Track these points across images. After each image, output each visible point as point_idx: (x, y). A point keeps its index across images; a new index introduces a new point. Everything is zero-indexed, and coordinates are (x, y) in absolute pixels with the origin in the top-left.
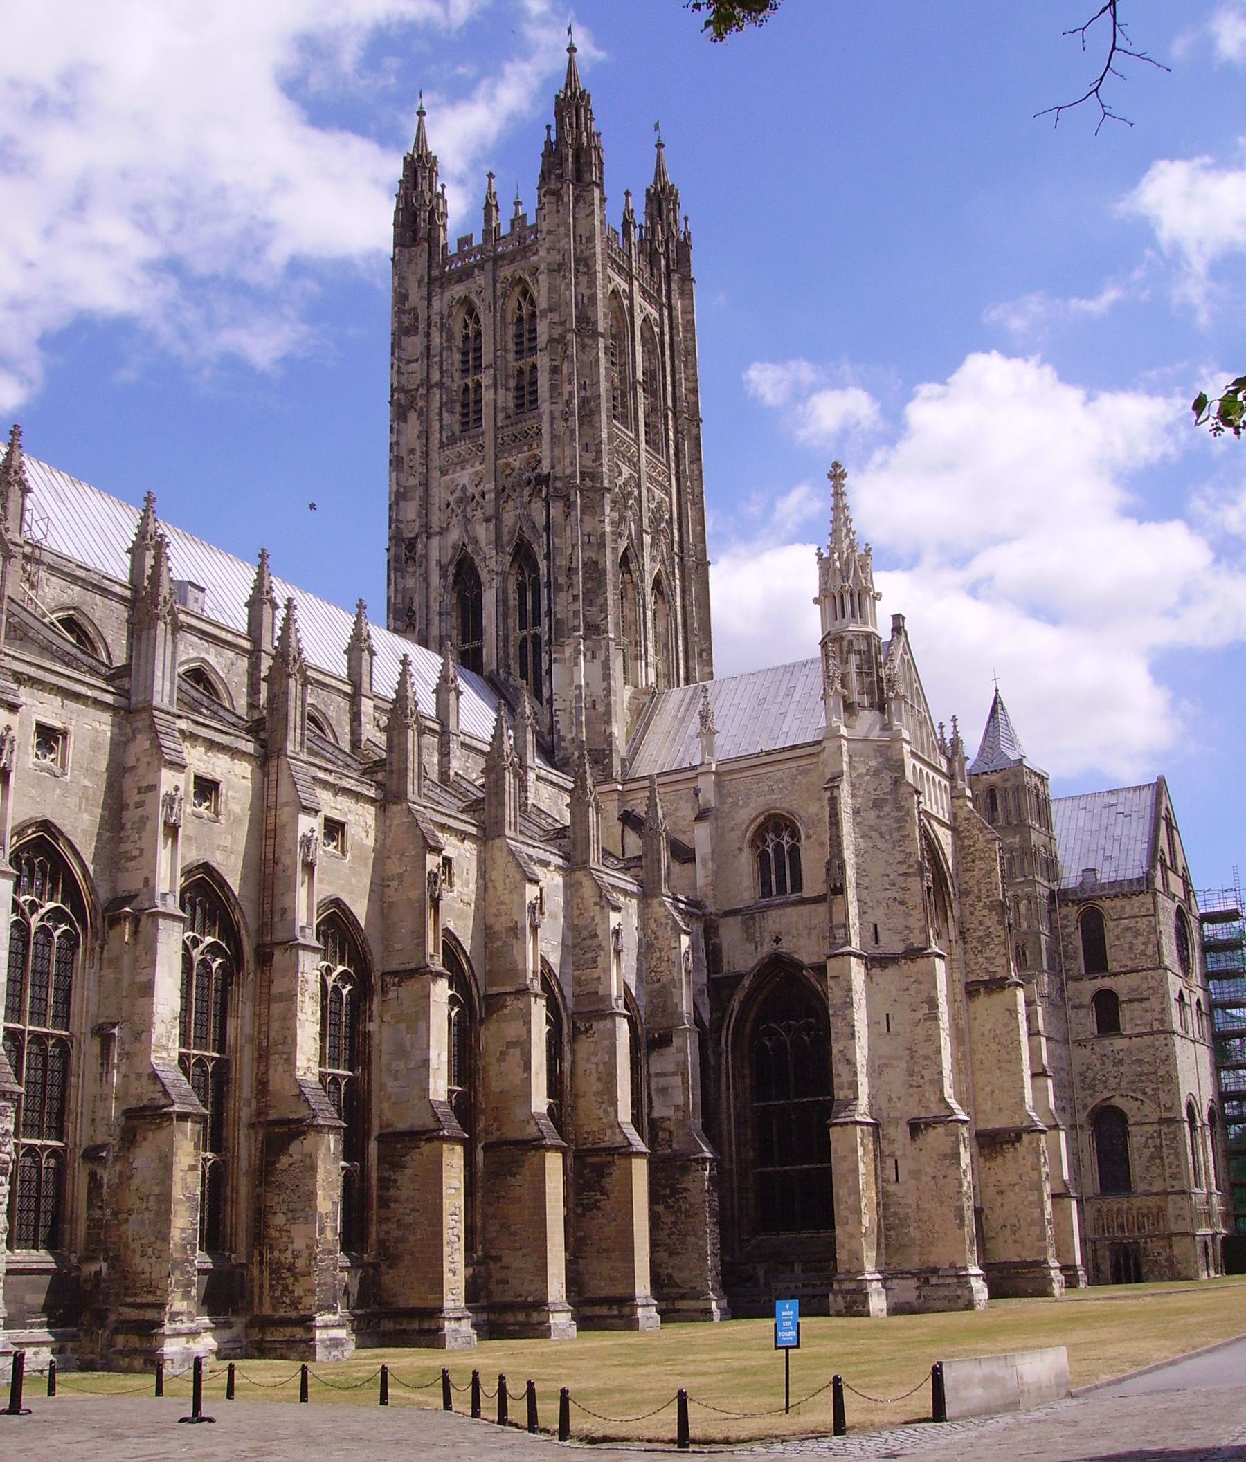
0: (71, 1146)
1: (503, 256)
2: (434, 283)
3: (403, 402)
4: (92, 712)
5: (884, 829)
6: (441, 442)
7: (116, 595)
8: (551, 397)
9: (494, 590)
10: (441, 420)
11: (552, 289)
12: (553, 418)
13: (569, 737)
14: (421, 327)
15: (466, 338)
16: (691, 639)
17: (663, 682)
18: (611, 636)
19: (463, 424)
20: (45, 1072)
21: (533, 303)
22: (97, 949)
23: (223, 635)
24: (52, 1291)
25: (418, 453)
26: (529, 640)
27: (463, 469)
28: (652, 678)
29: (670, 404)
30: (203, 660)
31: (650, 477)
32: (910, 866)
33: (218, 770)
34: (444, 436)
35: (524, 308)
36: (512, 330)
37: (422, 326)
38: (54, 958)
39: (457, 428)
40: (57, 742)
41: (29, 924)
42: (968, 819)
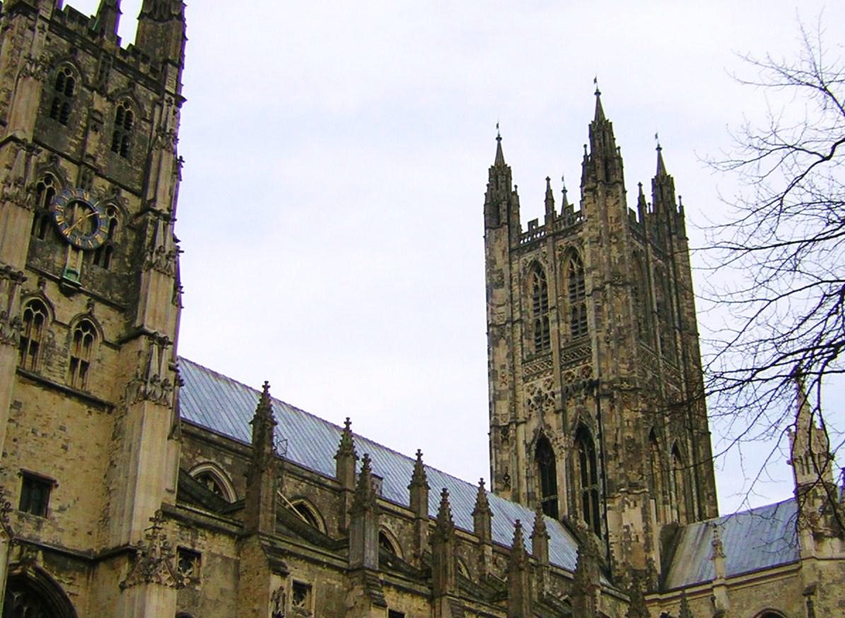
1: (559, 233)
2: (515, 251)
3: (495, 333)
6: (523, 360)
7: (328, 487)
8: (597, 327)
9: (564, 460)
10: (522, 345)
11: (593, 254)
12: (598, 343)
13: (621, 562)
14: (506, 282)
15: (536, 288)
16: (701, 486)
17: (683, 518)
18: (647, 490)
19: (537, 347)
21: (580, 263)
23: (396, 508)
25: (507, 367)
26: (590, 494)
27: (538, 377)
28: (676, 517)
29: (677, 325)
30: (384, 527)
31: (666, 376)
33: (404, 606)
35: (575, 267)
36: (567, 282)
37: (507, 282)
39: (533, 350)
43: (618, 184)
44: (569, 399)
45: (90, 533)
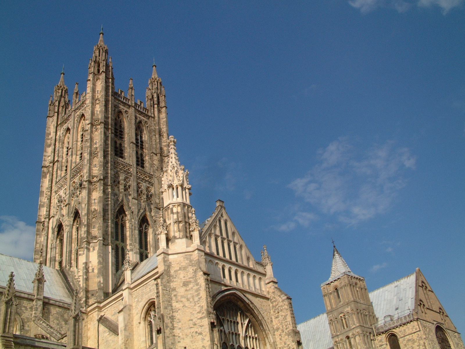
5: (189, 296)
6: (56, 181)
9: (66, 233)
10: (57, 174)
27: (61, 189)
32: (203, 313)
34: (58, 179)
37: (53, 142)
42: (273, 292)
43: (103, 73)
44: (73, 197)
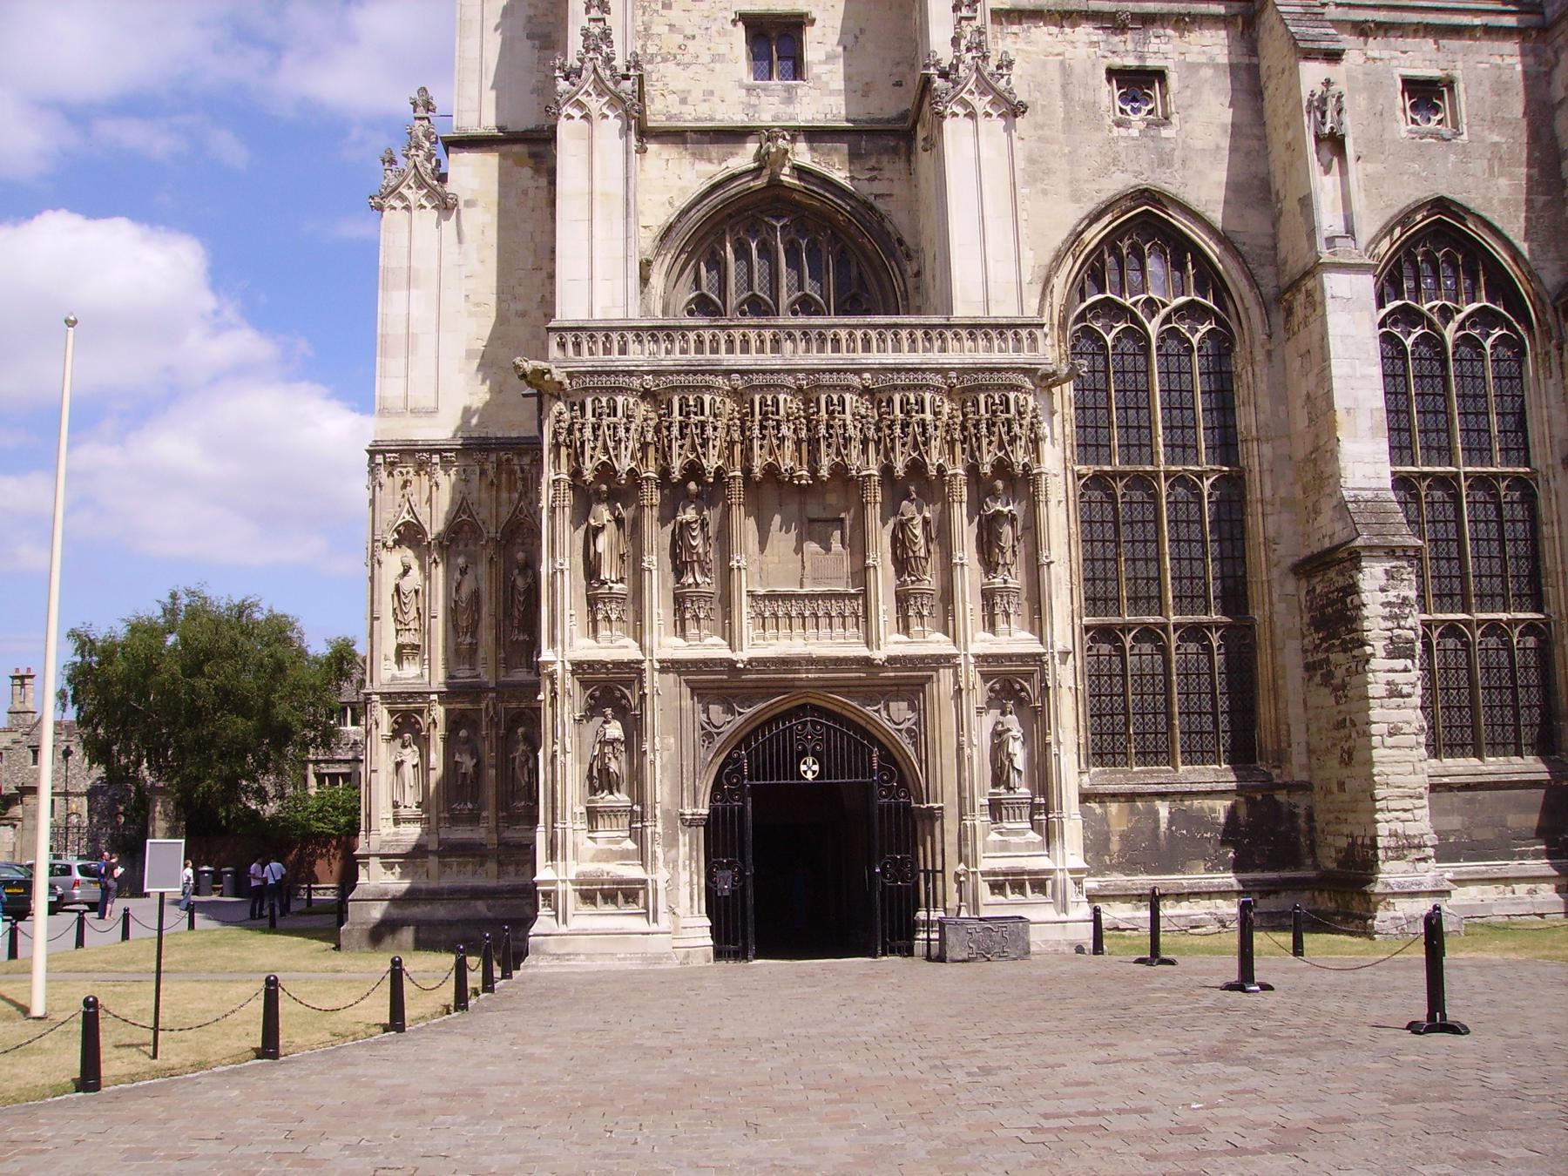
0: (1555, 617)
4: (1487, 46)
20: (1500, 524)
22: (1554, 352)
24: (1547, 810)
38: (1490, 375)
40: (1441, 98)
41: (1442, 336)
45: (899, 84)
